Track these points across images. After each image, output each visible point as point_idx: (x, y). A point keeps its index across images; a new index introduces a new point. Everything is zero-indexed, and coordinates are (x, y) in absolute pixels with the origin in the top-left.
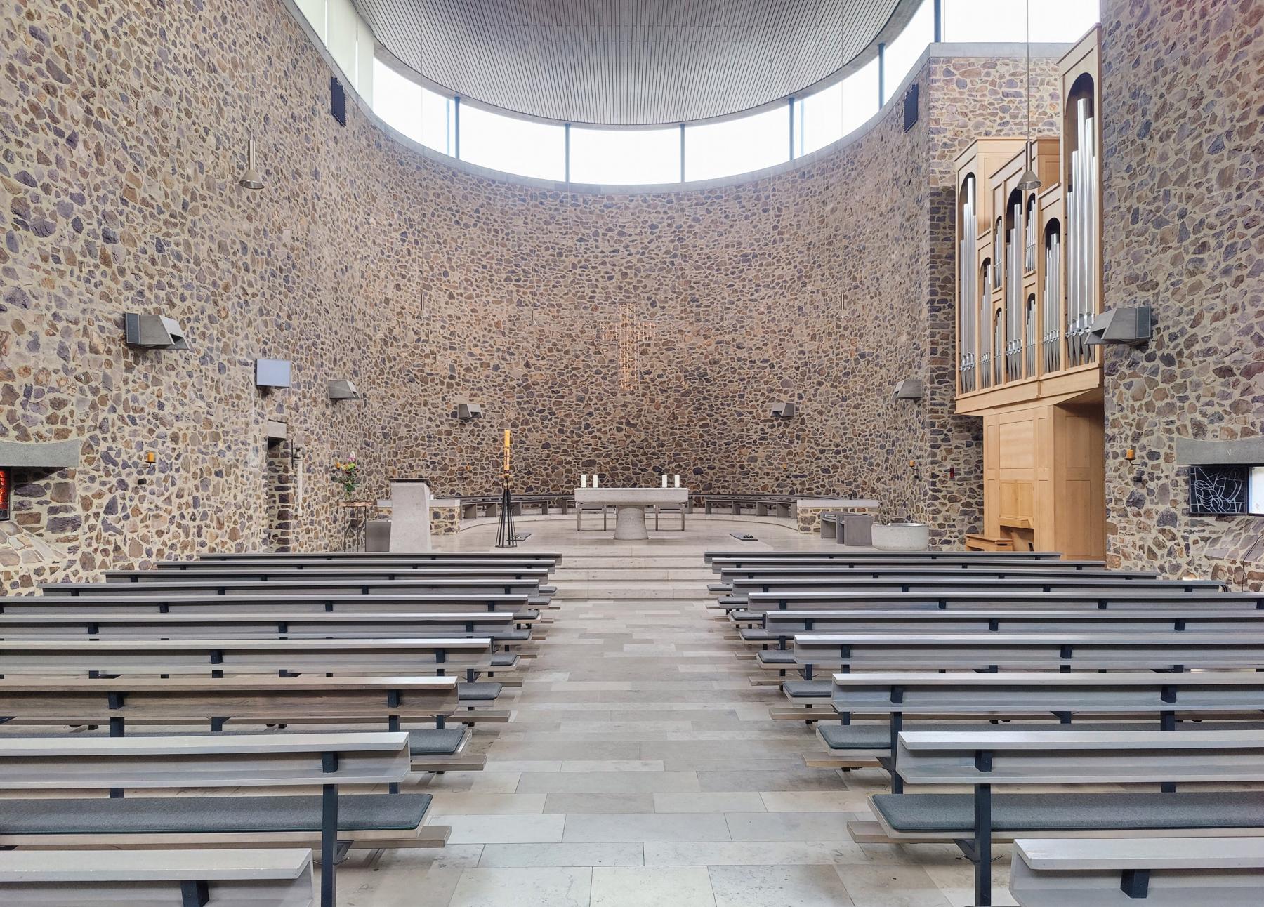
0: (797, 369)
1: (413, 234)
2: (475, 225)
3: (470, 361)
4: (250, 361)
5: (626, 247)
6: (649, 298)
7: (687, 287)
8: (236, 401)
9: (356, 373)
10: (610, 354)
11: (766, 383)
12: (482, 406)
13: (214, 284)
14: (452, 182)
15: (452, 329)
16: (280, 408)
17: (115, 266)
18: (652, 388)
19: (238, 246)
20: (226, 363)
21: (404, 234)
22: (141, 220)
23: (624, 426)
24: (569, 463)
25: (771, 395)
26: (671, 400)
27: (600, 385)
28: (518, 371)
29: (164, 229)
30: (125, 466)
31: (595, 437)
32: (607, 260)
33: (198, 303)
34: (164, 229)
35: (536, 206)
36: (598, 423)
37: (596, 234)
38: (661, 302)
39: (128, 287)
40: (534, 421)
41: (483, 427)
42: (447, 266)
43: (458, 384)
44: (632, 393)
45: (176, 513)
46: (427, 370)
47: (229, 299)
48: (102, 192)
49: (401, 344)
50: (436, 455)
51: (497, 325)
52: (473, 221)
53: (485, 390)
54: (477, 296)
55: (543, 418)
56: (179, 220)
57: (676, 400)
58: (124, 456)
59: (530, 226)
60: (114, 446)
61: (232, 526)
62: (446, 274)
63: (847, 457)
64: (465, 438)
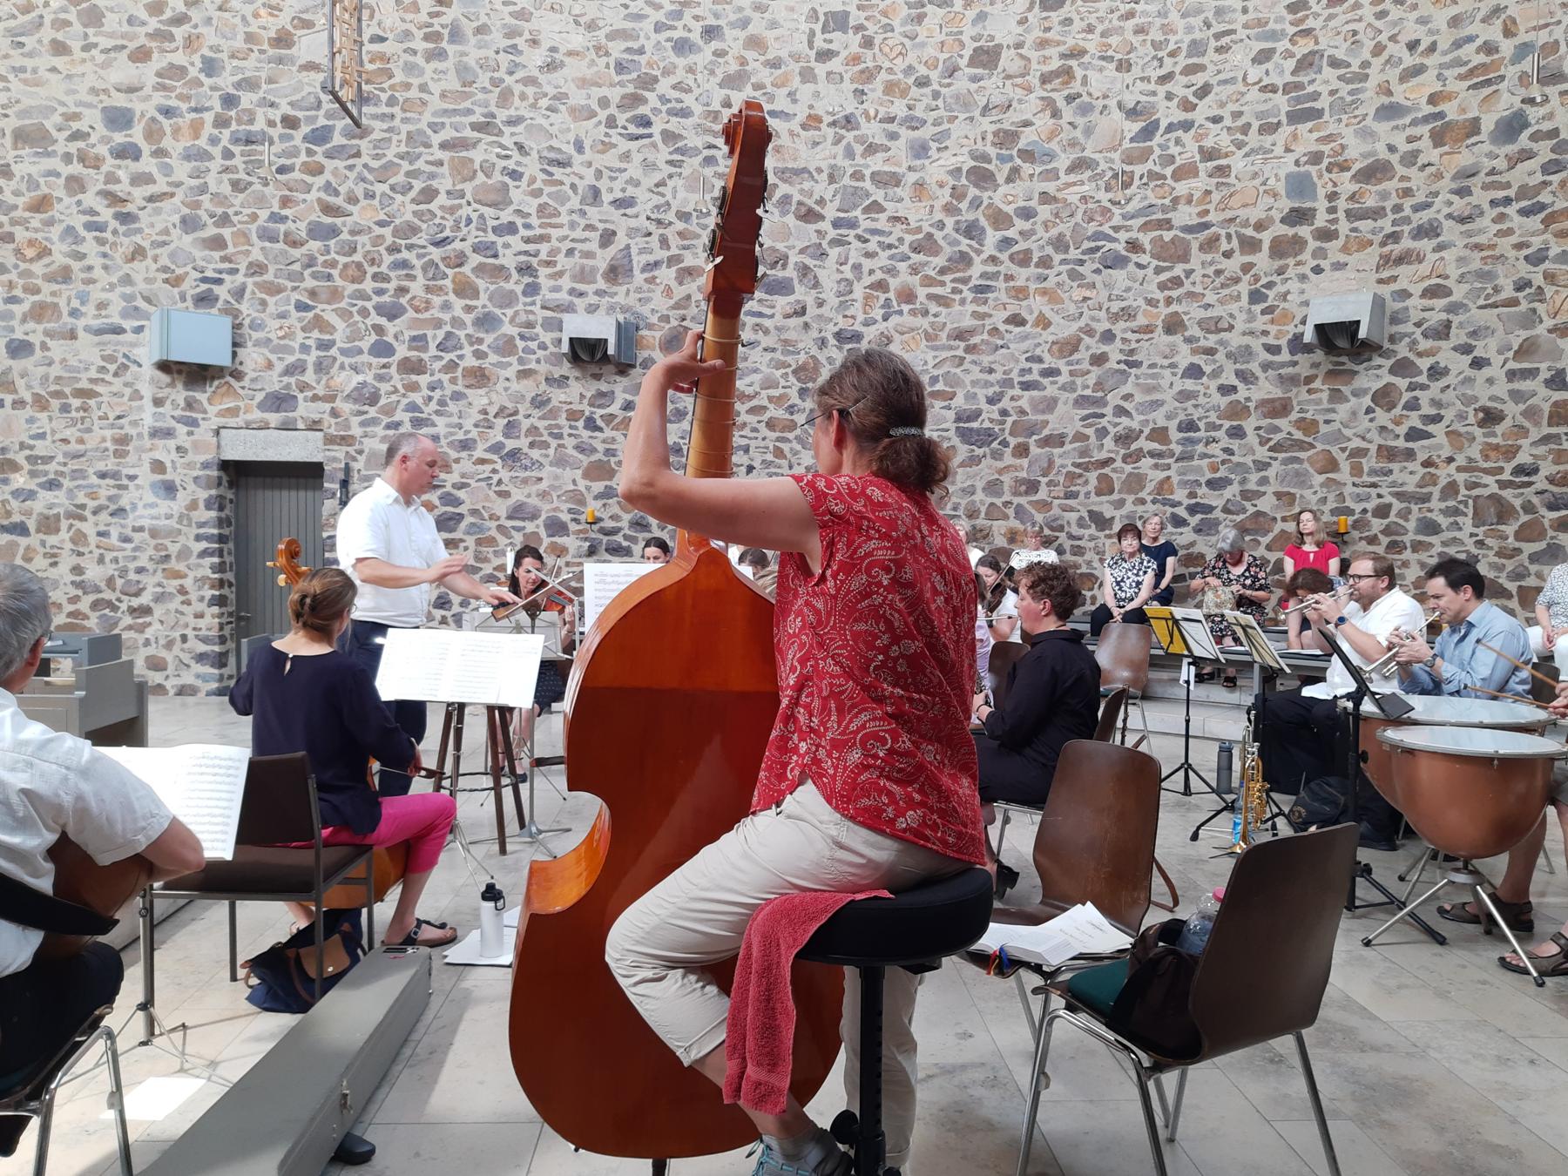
15: (1304, 47)
41: (1436, 372)
43: (1326, 235)
46: (1185, 215)
49: (1063, 162)
53: (1450, 231)
64: (1350, 414)
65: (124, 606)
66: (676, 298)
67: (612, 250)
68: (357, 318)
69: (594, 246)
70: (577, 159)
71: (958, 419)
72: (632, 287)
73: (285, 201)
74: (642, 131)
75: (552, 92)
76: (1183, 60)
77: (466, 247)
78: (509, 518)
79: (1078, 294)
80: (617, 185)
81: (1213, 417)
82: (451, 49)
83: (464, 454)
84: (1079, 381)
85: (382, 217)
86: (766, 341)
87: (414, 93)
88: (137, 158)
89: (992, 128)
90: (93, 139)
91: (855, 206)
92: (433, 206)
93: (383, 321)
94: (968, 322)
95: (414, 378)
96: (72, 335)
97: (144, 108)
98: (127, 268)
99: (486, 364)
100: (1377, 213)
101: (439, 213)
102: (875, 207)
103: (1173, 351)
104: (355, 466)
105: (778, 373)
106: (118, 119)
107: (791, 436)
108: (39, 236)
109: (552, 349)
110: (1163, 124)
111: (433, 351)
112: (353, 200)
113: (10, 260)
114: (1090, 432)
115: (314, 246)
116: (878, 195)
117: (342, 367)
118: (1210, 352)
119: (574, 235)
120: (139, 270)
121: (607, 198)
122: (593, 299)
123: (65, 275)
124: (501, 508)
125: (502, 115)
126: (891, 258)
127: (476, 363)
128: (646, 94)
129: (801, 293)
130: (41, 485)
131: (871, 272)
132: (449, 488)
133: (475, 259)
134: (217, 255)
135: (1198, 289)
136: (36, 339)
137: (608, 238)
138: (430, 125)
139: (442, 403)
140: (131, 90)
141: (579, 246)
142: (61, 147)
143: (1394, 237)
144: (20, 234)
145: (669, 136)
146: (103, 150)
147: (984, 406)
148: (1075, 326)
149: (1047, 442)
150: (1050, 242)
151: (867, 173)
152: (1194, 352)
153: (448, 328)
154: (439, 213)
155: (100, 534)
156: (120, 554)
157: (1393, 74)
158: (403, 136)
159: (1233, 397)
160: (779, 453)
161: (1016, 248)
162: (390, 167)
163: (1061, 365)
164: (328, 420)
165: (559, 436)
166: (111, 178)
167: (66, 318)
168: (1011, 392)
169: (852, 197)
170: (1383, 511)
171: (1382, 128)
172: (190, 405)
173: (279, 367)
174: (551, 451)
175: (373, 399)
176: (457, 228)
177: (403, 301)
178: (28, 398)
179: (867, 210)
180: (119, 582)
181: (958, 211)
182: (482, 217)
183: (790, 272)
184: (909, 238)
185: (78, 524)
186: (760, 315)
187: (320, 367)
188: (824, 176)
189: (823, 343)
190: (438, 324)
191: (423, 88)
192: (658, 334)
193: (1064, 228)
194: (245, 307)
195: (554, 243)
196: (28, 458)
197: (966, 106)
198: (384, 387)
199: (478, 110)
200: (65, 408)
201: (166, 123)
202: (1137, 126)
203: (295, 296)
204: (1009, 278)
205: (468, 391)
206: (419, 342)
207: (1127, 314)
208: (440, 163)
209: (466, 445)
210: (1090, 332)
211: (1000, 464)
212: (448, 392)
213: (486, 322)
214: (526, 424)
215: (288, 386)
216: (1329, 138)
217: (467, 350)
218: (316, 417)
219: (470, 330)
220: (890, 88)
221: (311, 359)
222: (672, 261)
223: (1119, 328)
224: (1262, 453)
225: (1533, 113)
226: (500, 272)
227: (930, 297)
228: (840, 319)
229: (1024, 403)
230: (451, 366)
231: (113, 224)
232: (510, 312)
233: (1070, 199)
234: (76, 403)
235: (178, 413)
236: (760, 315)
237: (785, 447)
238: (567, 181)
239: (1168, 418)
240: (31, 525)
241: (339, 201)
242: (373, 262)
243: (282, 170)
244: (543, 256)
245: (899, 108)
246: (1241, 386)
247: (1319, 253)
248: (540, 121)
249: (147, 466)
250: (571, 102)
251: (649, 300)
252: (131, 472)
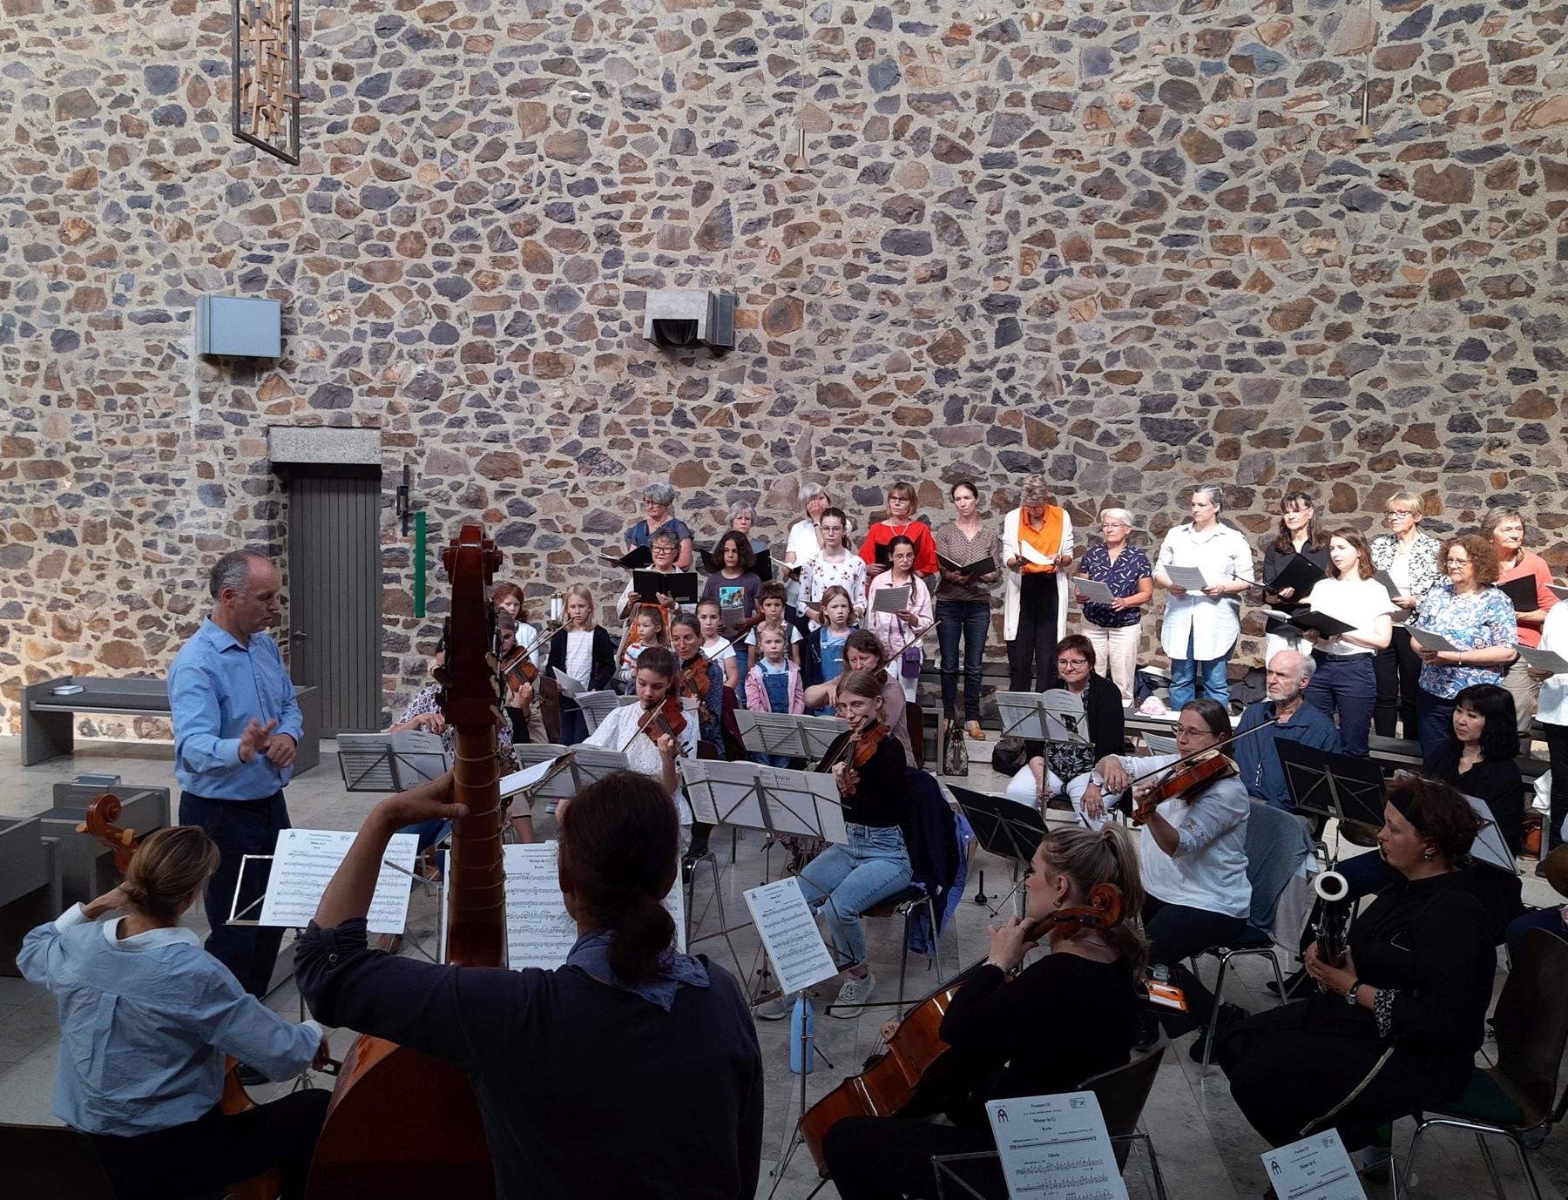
49: (1293, 69)
65: (171, 625)
66: (785, 262)
67: (707, 208)
68: (417, 298)
69: (685, 203)
70: (667, 98)
71: (1145, 408)
72: (733, 250)
73: (338, 166)
74: (745, 59)
75: (636, 17)
77: (537, 210)
78: (585, 530)
79: (1310, 245)
80: (717, 125)
81: (1500, 413)
83: (535, 456)
84: (1310, 361)
85: (444, 178)
86: (895, 313)
87: (478, 30)
88: (181, 124)
89: (1194, 29)
90: (137, 105)
91: (1012, 140)
92: (500, 164)
93: (444, 301)
94: (1159, 283)
95: (480, 367)
96: (117, 324)
97: (187, 65)
98: (171, 248)
99: (561, 349)
101: (507, 171)
102: (1039, 139)
103: (1444, 321)
104: (417, 469)
105: (910, 352)
106: (162, 79)
107: (924, 430)
108: (83, 215)
109: (636, 329)
110: (1438, 13)
111: (501, 335)
112: (410, 160)
113: (55, 243)
114: (1324, 427)
115: (369, 215)
116: (1042, 123)
117: (400, 356)
118: (1499, 323)
119: (663, 191)
120: (185, 249)
121: (702, 144)
122: (684, 268)
123: (107, 258)
124: (577, 518)
125: (579, 49)
126: (1058, 203)
127: (549, 349)
128: (751, 13)
129: (941, 251)
130: (86, 490)
131: (1032, 221)
132: (518, 495)
133: (548, 225)
134: (265, 229)
135: (1483, 238)
136: (80, 329)
137: (702, 193)
138: (497, 67)
139: (511, 396)
140: (175, 46)
141: (668, 204)
142: (104, 116)
144: (65, 213)
145: (777, 64)
146: (146, 116)
147: (1180, 392)
148: (1305, 288)
149: (1264, 439)
150: (1273, 177)
151: (1028, 95)
152: (1475, 323)
153: (517, 307)
154: (507, 171)
155: (146, 544)
156: (167, 567)
158: (467, 82)
159: (1530, 386)
160: (909, 451)
161: (1225, 186)
162: (452, 120)
163: (1286, 339)
164: (386, 417)
165: (644, 434)
166: (156, 147)
167: (111, 306)
168: (1217, 374)
169: (1008, 127)
172: (238, 400)
173: (332, 356)
174: (634, 451)
175: (435, 393)
176: (527, 188)
177: (468, 277)
178: (74, 395)
179: (1026, 143)
180: (167, 597)
181: (1148, 140)
182: (555, 174)
183: (927, 226)
184: (1081, 177)
185: (124, 533)
186: (888, 280)
187: (377, 356)
188: (972, 102)
189: (966, 313)
190: (507, 303)
191: (489, 23)
192: (761, 308)
193: (1294, 158)
194: (295, 289)
195: (640, 202)
196: (74, 460)
198: (447, 378)
199: (552, 45)
200: (111, 405)
201: (211, 81)
203: (349, 274)
204: (1216, 225)
205: (539, 382)
206: (485, 325)
207: (1380, 271)
208: (507, 112)
209: (537, 445)
210: (1326, 296)
211: (1200, 467)
212: (517, 383)
213: (562, 299)
214: (605, 419)
215: (342, 378)
217: (539, 334)
218: (373, 413)
219: (542, 310)
221: (366, 347)
222: (781, 217)
223: (1367, 291)
226: (575, 240)
227: (1109, 251)
228: (990, 282)
229: (1234, 388)
230: (521, 353)
231: (158, 198)
232: (587, 287)
233: (1302, 119)
234: (121, 399)
235: (226, 409)
236: (888, 280)
237: (917, 444)
238: (655, 126)
239: (1436, 411)
240: (78, 533)
241: (396, 162)
242: (433, 232)
243: (333, 129)
244: (626, 218)
246: (1542, 371)
248: (623, 54)
249: (194, 470)
250: (660, 28)
251: (751, 267)
252: (178, 475)
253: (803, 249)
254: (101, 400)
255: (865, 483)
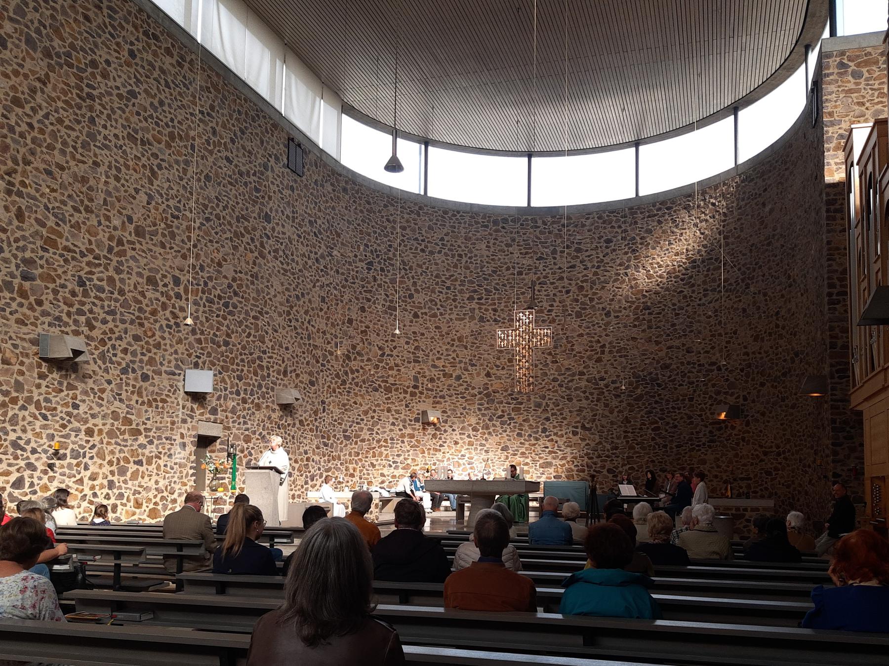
0: (742, 370)
1: (379, 263)
2: (440, 252)
3: (434, 373)
4: (177, 372)
5: (581, 262)
6: (604, 309)
7: (640, 296)
8: (161, 405)
9: (312, 383)
10: (566, 363)
11: (714, 386)
12: (444, 412)
13: (140, 310)
14: (419, 215)
15: (416, 344)
16: (214, 411)
17: (32, 299)
18: (606, 394)
19: (169, 280)
20: (150, 373)
21: (370, 263)
22: (62, 263)
23: (579, 430)
24: (527, 464)
25: (719, 398)
26: (624, 404)
27: (556, 391)
28: (479, 381)
29: (87, 269)
30: (34, 451)
31: (552, 440)
32: (565, 275)
33: (122, 326)
34: (87, 269)
35: (497, 231)
36: (555, 427)
37: (554, 252)
38: (615, 311)
39: (45, 314)
40: (494, 425)
41: (445, 431)
42: (413, 289)
43: (421, 393)
44: (587, 398)
45: (89, 493)
46: (391, 380)
47: (156, 321)
48: (21, 244)
49: (365, 358)
50: (398, 456)
51: (460, 339)
52: (438, 248)
54: (441, 314)
55: (503, 423)
56: (103, 261)
57: (629, 404)
58: (33, 444)
59: (492, 249)
60: (23, 436)
61: (151, 506)
62: (411, 296)
63: (786, 459)
67: (283, 365)
76: (390, 338)
82: (256, 282)
100: (432, 390)
116: (329, 358)
133: (258, 362)
143: (436, 397)
157: (435, 357)
170: (435, 464)
171: (432, 369)
193: (365, 377)
197: (346, 335)
202: (380, 353)
207: (378, 405)
216: (421, 369)
220: (332, 324)
222: (295, 370)
224: (408, 448)
225: (463, 376)
245: (333, 331)
247: (420, 397)
253: (297, 381)
254: (154, 404)
255: (305, 448)
